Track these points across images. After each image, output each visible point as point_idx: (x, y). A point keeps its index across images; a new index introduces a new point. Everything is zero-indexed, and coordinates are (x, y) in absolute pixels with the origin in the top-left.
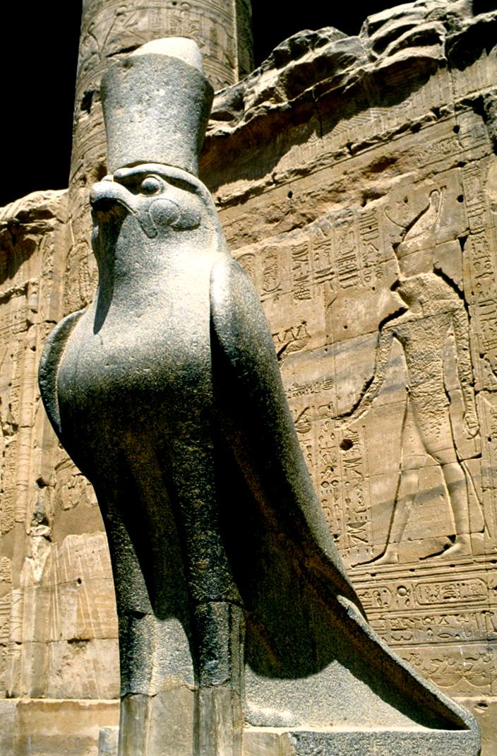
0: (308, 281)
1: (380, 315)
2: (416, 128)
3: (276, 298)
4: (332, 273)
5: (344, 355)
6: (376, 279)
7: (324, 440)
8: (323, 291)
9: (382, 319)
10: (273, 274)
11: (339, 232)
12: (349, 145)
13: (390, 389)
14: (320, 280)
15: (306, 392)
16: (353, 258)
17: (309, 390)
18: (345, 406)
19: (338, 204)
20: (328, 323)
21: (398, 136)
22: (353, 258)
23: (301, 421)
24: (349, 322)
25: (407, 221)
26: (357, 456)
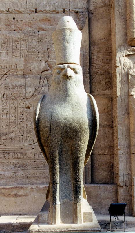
2: (58, 12)
4: (27, 51)
5: (29, 79)
7: (20, 105)
8: (23, 56)
10: (6, 44)
11: (30, 38)
12: (36, 10)
14: (23, 52)
16: (34, 48)
17: (17, 88)
19: (29, 28)
21: (52, 13)
22: (34, 48)
23: (13, 97)
24: (32, 69)
26: (31, 112)
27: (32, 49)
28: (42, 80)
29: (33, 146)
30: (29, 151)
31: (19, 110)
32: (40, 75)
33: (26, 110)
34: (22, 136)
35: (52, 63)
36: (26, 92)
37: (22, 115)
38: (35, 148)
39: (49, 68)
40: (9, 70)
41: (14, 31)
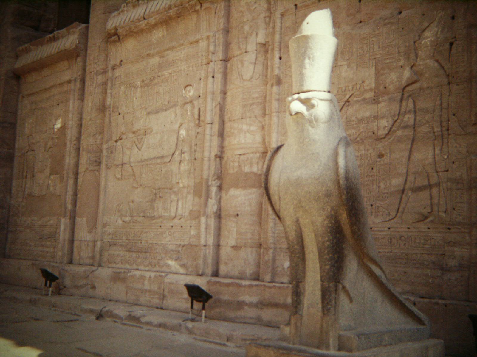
0: (367, 57)
1: (404, 83)
3: (348, 66)
5: (383, 104)
6: (403, 61)
8: (374, 64)
9: (404, 85)
13: (406, 127)
15: (362, 123)
17: (364, 122)
18: (382, 132)
20: (376, 84)
25: (424, 27)
26: (385, 162)
27: (387, 49)
28: (404, 103)
29: (388, 225)
30: (384, 233)
31: (367, 161)
32: (400, 94)
33: (379, 160)
34: (372, 205)
35: (422, 67)
36: (378, 129)
37: (372, 169)
38: (392, 227)
39: (416, 78)
40: (353, 92)
41: (361, 22)
